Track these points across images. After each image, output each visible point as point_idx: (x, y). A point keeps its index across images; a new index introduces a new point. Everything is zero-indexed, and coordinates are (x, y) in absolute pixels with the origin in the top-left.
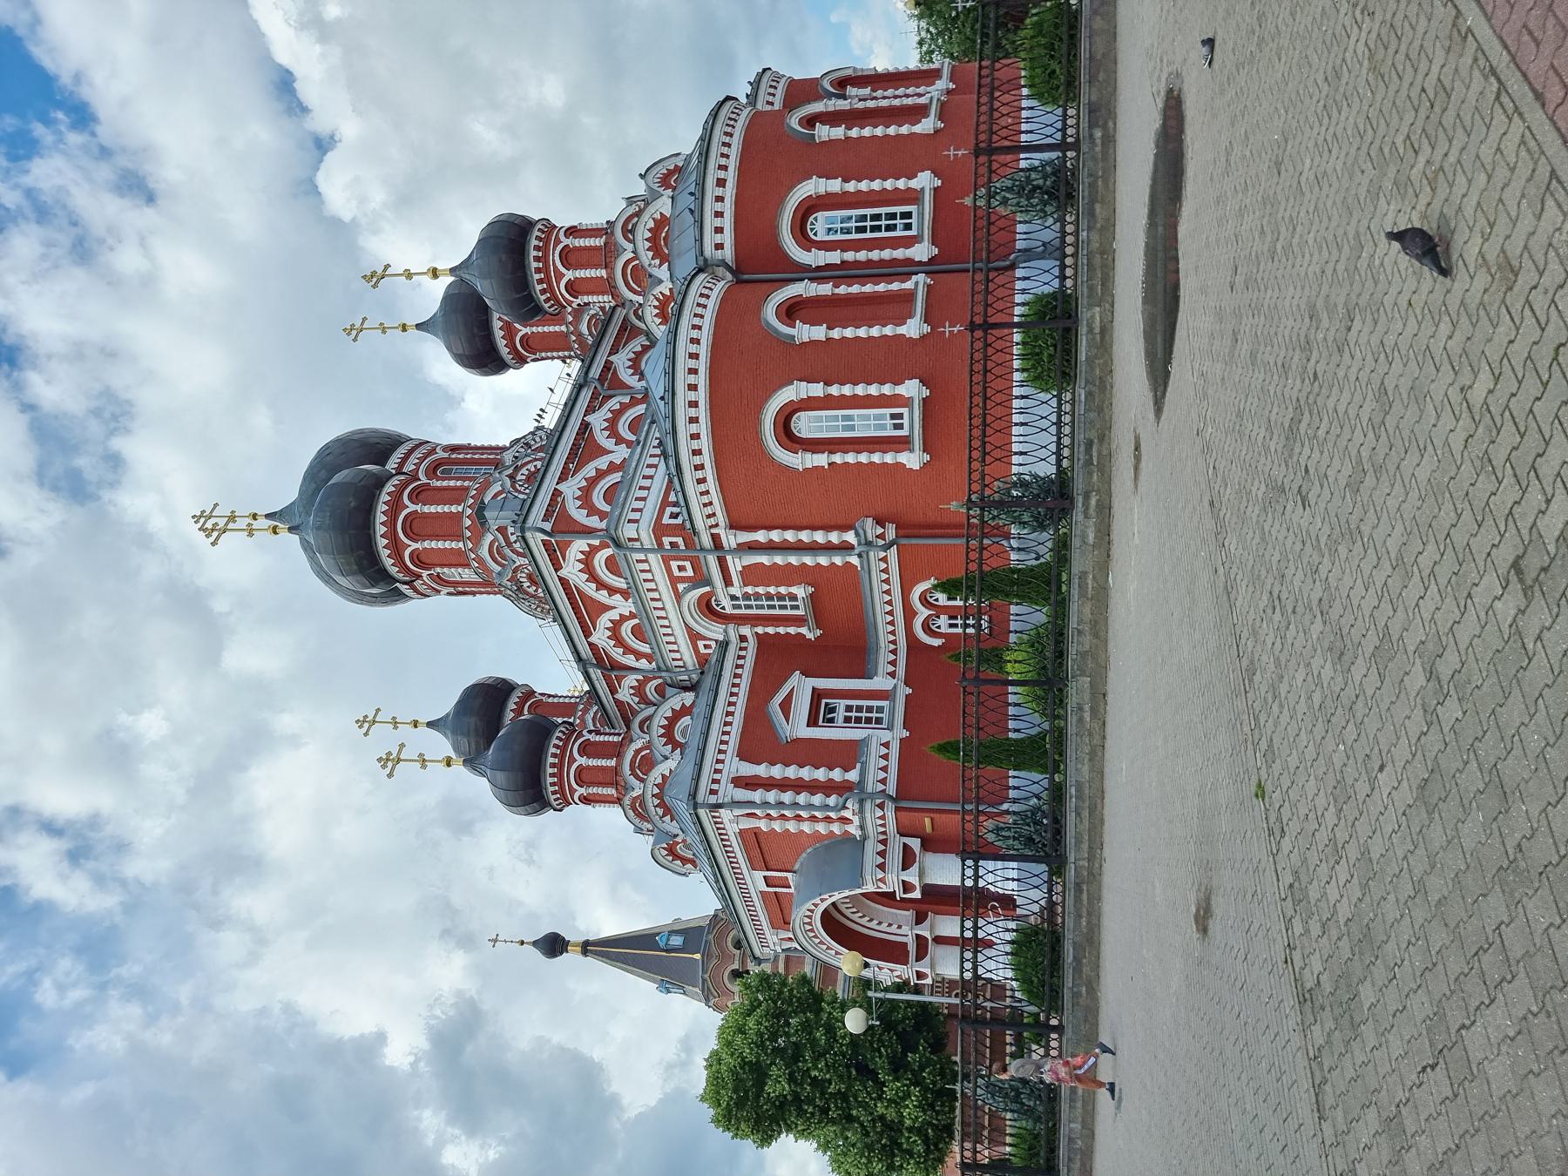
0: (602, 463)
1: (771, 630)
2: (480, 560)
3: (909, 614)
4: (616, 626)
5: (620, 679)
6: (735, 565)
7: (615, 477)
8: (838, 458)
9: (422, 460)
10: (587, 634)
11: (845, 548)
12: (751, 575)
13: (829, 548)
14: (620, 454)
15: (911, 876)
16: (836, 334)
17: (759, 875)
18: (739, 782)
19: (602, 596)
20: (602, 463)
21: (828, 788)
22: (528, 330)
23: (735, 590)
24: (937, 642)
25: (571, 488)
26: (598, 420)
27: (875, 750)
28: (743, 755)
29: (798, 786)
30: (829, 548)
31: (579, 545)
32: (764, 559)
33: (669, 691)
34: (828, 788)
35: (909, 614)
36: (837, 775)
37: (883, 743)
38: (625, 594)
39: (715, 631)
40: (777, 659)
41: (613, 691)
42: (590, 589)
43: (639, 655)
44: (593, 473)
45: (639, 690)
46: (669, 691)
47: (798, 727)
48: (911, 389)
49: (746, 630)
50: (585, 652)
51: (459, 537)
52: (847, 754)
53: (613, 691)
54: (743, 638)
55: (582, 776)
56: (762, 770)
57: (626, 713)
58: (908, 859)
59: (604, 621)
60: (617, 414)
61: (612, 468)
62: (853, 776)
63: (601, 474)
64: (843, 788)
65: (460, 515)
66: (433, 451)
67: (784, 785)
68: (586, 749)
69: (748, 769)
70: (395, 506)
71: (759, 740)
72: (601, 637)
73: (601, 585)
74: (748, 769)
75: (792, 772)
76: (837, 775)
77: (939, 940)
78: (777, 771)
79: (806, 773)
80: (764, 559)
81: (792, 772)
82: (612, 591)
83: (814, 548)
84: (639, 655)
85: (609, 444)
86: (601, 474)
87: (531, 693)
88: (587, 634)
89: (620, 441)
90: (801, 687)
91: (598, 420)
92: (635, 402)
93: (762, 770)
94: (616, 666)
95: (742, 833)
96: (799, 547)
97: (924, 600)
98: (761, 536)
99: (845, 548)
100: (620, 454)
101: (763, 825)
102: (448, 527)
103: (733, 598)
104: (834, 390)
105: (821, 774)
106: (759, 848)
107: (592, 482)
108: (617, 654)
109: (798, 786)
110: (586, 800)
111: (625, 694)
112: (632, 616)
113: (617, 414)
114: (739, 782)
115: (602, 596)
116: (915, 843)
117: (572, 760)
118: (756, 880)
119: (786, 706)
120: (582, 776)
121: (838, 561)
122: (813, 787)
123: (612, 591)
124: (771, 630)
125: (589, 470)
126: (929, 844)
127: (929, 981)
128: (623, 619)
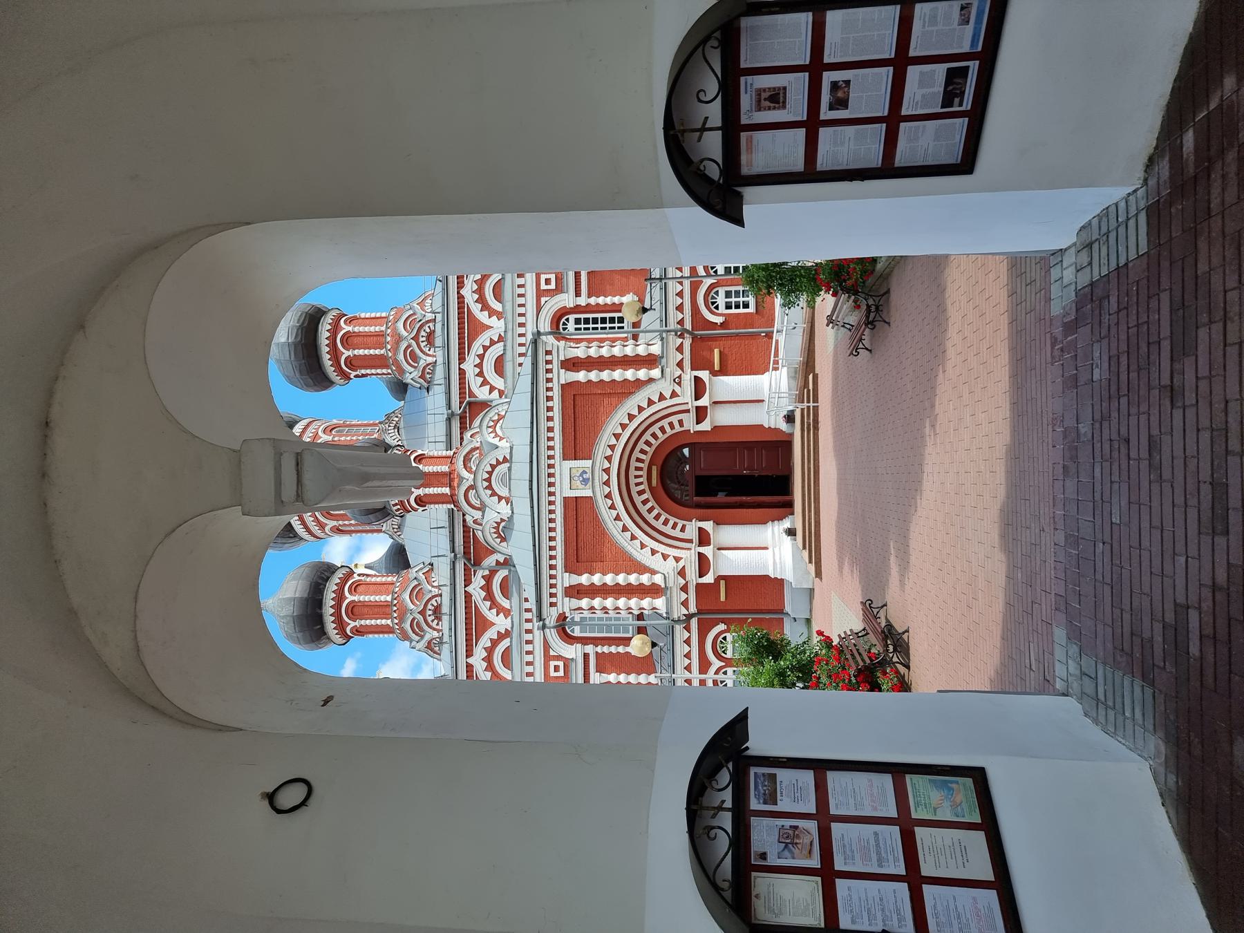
0: (491, 633)
1: (606, 649)
7: (505, 643)
14: (501, 623)
20: (491, 633)
22: (350, 353)
39: (572, 651)
44: (489, 644)
49: (590, 649)
61: (501, 637)
63: (495, 643)
86: (495, 643)
107: (490, 651)
113: (488, 579)
124: (606, 649)
125: (485, 641)
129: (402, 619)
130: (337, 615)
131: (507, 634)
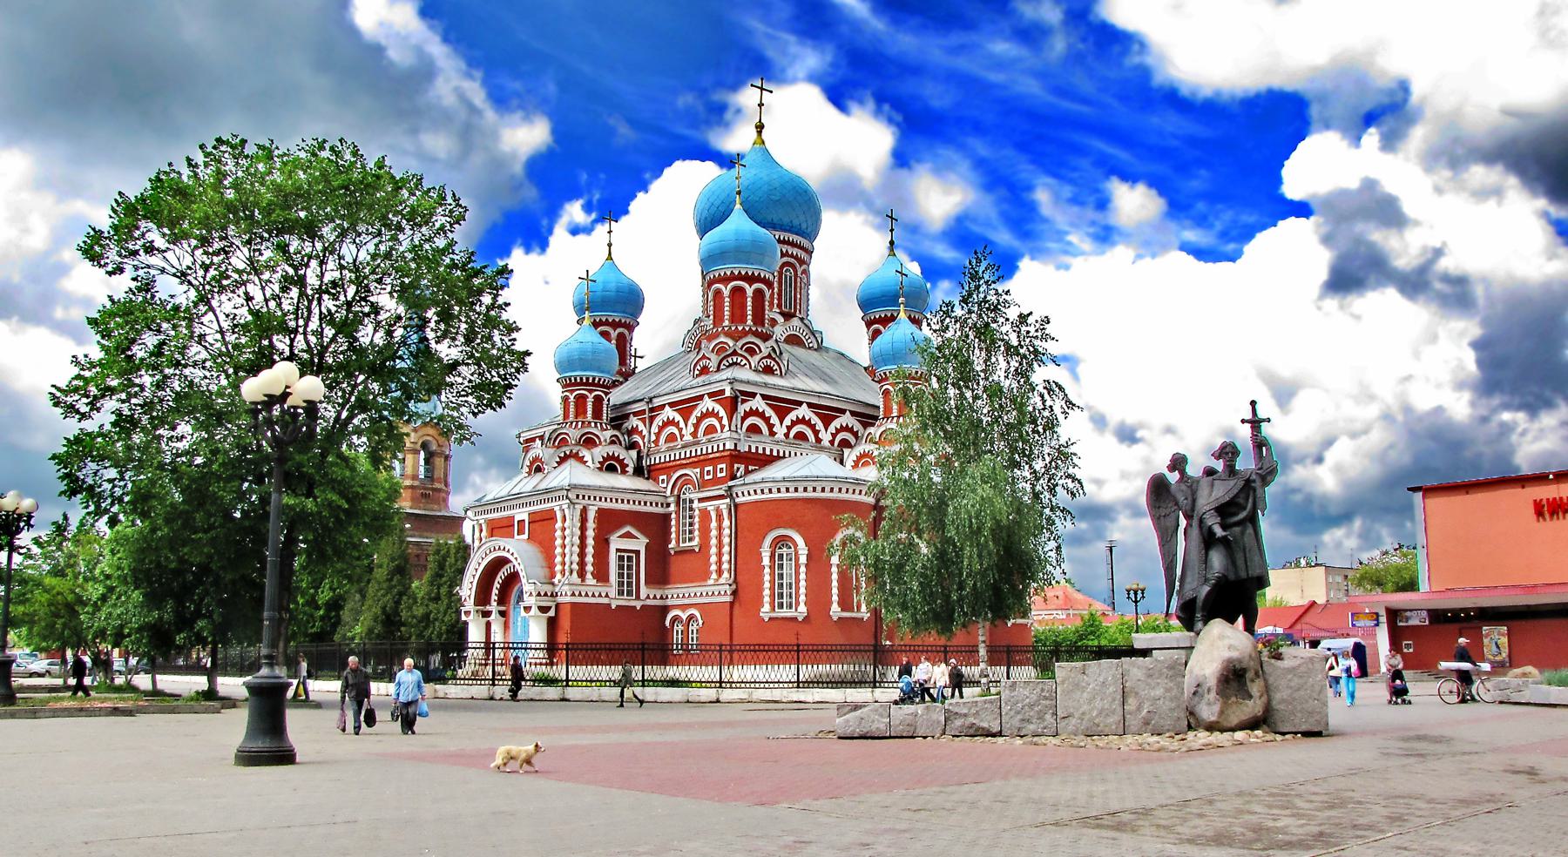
0: (775, 420)
2: (716, 336)
3: (684, 607)
4: (677, 425)
5: (643, 420)
6: (710, 506)
8: (767, 570)
9: (796, 258)
10: (672, 405)
11: (720, 572)
12: (705, 514)
13: (720, 562)
14: (780, 431)
15: (534, 611)
16: (834, 569)
17: (525, 517)
18: (584, 511)
19: (693, 420)
20: (775, 420)
21: (582, 564)
23: (696, 505)
24: (667, 623)
25: (758, 403)
26: (803, 411)
27: (604, 590)
28: (601, 512)
29: (583, 546)
30: (720, 562)
31: (722, 413)
32: (714, 524)
33: (634, 453)
34: (582, 564)
35: (684, 607)
36: (590, 568)
37: (610, 594)
38: (694, 434)
40: (656, 526)
41: (635, 414)
42: (697, 413)
43: (658, 435)
45: (634, 431)
46: (634, 453)
47: (616, 543)
48: (803, 608)
49: (673, 508)
50: (657, 402)
51: (732, 321)
52: (602, 575)
53: (635, 414)
54: (668, 505)
55: (581, 400)
56: (591, 525)
57: (618, 421)
58: (544, 609)
59: (678, 418)
60: (808, 423)
61: (771, 427)
62: (590, 579)
63: (767, 420)
64: (582, 574)
65: (743, 320)
66: (802, 262)
67: (583, 538)
68: (598, 400)
69: (591, 515)
70: (751, 279)
71: (610, 521)
72: (669, 413)
73: (699, 420)
74: (591, 515)
75: (590, 542)
76: (590, 568)
77: (488, 625)
78: (590, 533)
79: (590, 550)
80: (714, 524)
81: (590, 542)
82: (696, 426)
83: (720, 555)
84: (658, 435)
85: (787, 422)
87: (631, 328)
88: (672, 405)
89: (789, 428)
90: (640, 543)
91: (803, 411)
92: (816, 433)
93: (591, 525)
94: (652, 419)
95: (552, 510)
96: (720, 546)
97: (691, 617)
98: (726, 523)
99: (720, 572)
100: (780, 431)
101: (559, 525)
102: (739, 316)
103: (691, 501)
104: (803, 569)
105: (589, 559)
106: (543, 521)
107: (762, 415)
108: (658, 421)
109: (583, 546)
110: (565, 400)
111: (634, 422)
112: (682, 436)
114: (584, 511)
115: (693, 420)
116: (552, 613)
117: (590, 391)
118: (522, 515)
119: (628, 535)
120: (581, 400)
121: (714, 567)
122: (582, 555)
123: (696, 426)
125: (769, 412)
126: (552, 625)
127: (464, 618)
128: (680, 430)
129: (727, 334)
130: (733, 278)
131: (772, 434)
